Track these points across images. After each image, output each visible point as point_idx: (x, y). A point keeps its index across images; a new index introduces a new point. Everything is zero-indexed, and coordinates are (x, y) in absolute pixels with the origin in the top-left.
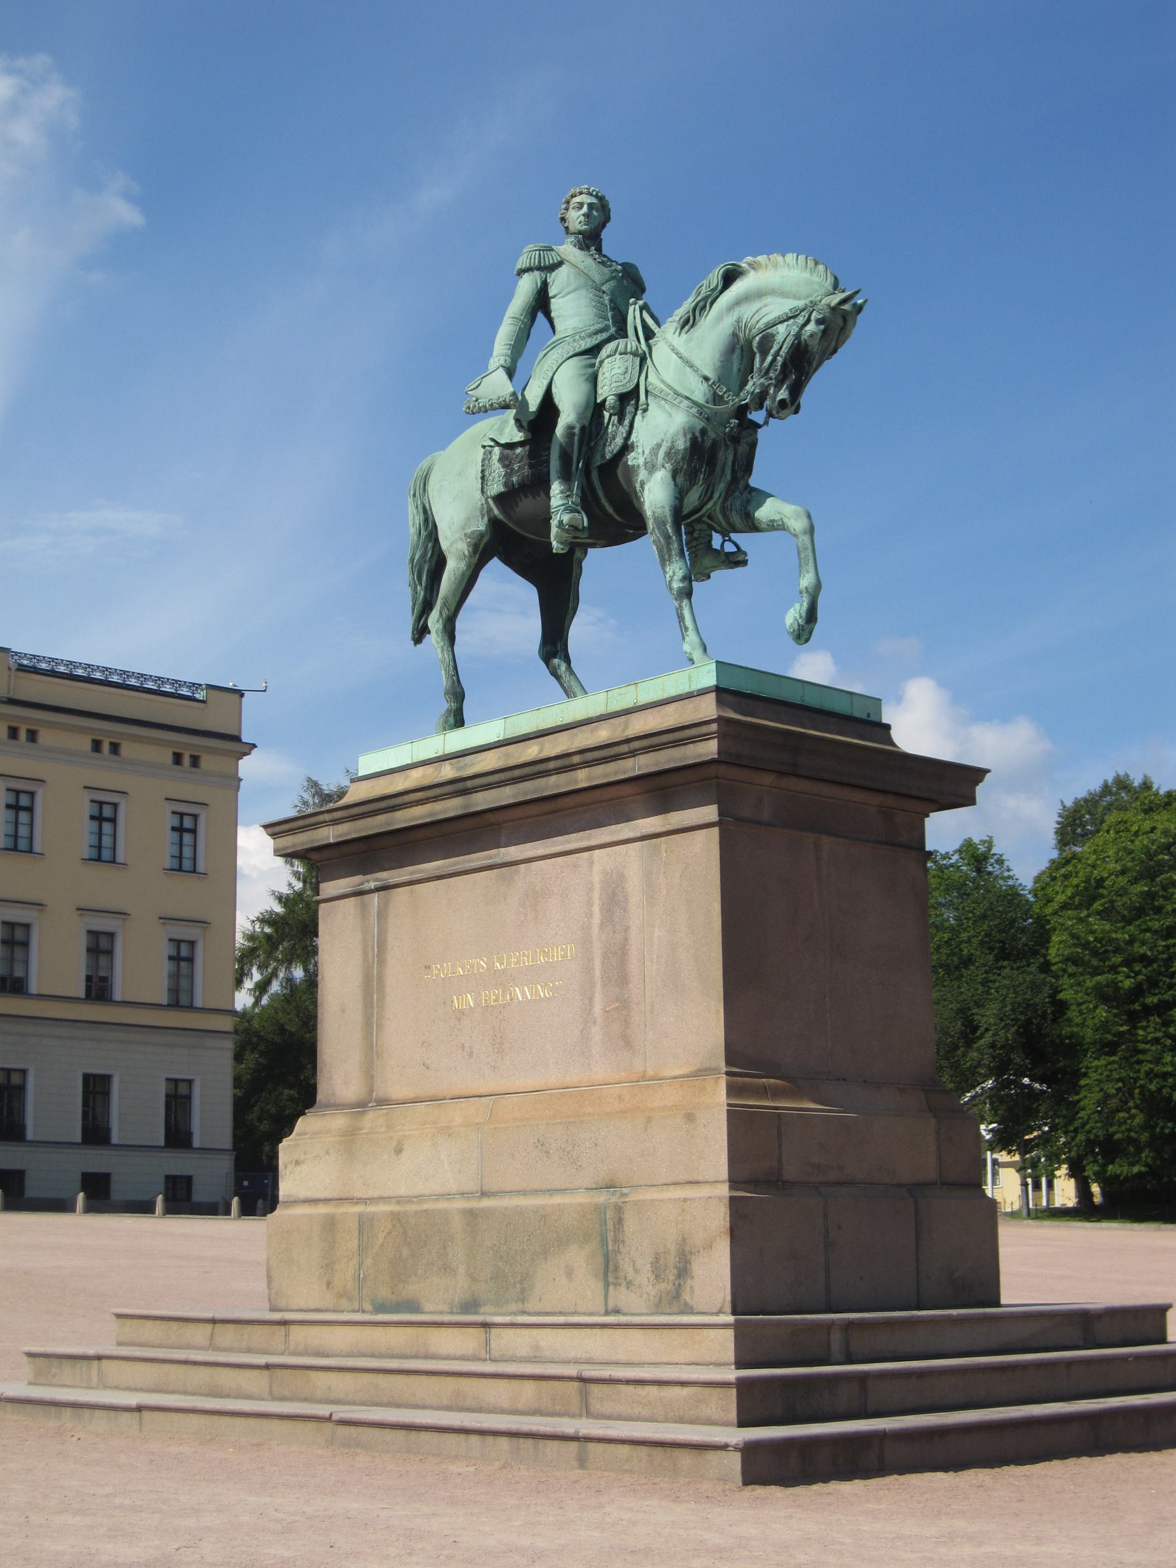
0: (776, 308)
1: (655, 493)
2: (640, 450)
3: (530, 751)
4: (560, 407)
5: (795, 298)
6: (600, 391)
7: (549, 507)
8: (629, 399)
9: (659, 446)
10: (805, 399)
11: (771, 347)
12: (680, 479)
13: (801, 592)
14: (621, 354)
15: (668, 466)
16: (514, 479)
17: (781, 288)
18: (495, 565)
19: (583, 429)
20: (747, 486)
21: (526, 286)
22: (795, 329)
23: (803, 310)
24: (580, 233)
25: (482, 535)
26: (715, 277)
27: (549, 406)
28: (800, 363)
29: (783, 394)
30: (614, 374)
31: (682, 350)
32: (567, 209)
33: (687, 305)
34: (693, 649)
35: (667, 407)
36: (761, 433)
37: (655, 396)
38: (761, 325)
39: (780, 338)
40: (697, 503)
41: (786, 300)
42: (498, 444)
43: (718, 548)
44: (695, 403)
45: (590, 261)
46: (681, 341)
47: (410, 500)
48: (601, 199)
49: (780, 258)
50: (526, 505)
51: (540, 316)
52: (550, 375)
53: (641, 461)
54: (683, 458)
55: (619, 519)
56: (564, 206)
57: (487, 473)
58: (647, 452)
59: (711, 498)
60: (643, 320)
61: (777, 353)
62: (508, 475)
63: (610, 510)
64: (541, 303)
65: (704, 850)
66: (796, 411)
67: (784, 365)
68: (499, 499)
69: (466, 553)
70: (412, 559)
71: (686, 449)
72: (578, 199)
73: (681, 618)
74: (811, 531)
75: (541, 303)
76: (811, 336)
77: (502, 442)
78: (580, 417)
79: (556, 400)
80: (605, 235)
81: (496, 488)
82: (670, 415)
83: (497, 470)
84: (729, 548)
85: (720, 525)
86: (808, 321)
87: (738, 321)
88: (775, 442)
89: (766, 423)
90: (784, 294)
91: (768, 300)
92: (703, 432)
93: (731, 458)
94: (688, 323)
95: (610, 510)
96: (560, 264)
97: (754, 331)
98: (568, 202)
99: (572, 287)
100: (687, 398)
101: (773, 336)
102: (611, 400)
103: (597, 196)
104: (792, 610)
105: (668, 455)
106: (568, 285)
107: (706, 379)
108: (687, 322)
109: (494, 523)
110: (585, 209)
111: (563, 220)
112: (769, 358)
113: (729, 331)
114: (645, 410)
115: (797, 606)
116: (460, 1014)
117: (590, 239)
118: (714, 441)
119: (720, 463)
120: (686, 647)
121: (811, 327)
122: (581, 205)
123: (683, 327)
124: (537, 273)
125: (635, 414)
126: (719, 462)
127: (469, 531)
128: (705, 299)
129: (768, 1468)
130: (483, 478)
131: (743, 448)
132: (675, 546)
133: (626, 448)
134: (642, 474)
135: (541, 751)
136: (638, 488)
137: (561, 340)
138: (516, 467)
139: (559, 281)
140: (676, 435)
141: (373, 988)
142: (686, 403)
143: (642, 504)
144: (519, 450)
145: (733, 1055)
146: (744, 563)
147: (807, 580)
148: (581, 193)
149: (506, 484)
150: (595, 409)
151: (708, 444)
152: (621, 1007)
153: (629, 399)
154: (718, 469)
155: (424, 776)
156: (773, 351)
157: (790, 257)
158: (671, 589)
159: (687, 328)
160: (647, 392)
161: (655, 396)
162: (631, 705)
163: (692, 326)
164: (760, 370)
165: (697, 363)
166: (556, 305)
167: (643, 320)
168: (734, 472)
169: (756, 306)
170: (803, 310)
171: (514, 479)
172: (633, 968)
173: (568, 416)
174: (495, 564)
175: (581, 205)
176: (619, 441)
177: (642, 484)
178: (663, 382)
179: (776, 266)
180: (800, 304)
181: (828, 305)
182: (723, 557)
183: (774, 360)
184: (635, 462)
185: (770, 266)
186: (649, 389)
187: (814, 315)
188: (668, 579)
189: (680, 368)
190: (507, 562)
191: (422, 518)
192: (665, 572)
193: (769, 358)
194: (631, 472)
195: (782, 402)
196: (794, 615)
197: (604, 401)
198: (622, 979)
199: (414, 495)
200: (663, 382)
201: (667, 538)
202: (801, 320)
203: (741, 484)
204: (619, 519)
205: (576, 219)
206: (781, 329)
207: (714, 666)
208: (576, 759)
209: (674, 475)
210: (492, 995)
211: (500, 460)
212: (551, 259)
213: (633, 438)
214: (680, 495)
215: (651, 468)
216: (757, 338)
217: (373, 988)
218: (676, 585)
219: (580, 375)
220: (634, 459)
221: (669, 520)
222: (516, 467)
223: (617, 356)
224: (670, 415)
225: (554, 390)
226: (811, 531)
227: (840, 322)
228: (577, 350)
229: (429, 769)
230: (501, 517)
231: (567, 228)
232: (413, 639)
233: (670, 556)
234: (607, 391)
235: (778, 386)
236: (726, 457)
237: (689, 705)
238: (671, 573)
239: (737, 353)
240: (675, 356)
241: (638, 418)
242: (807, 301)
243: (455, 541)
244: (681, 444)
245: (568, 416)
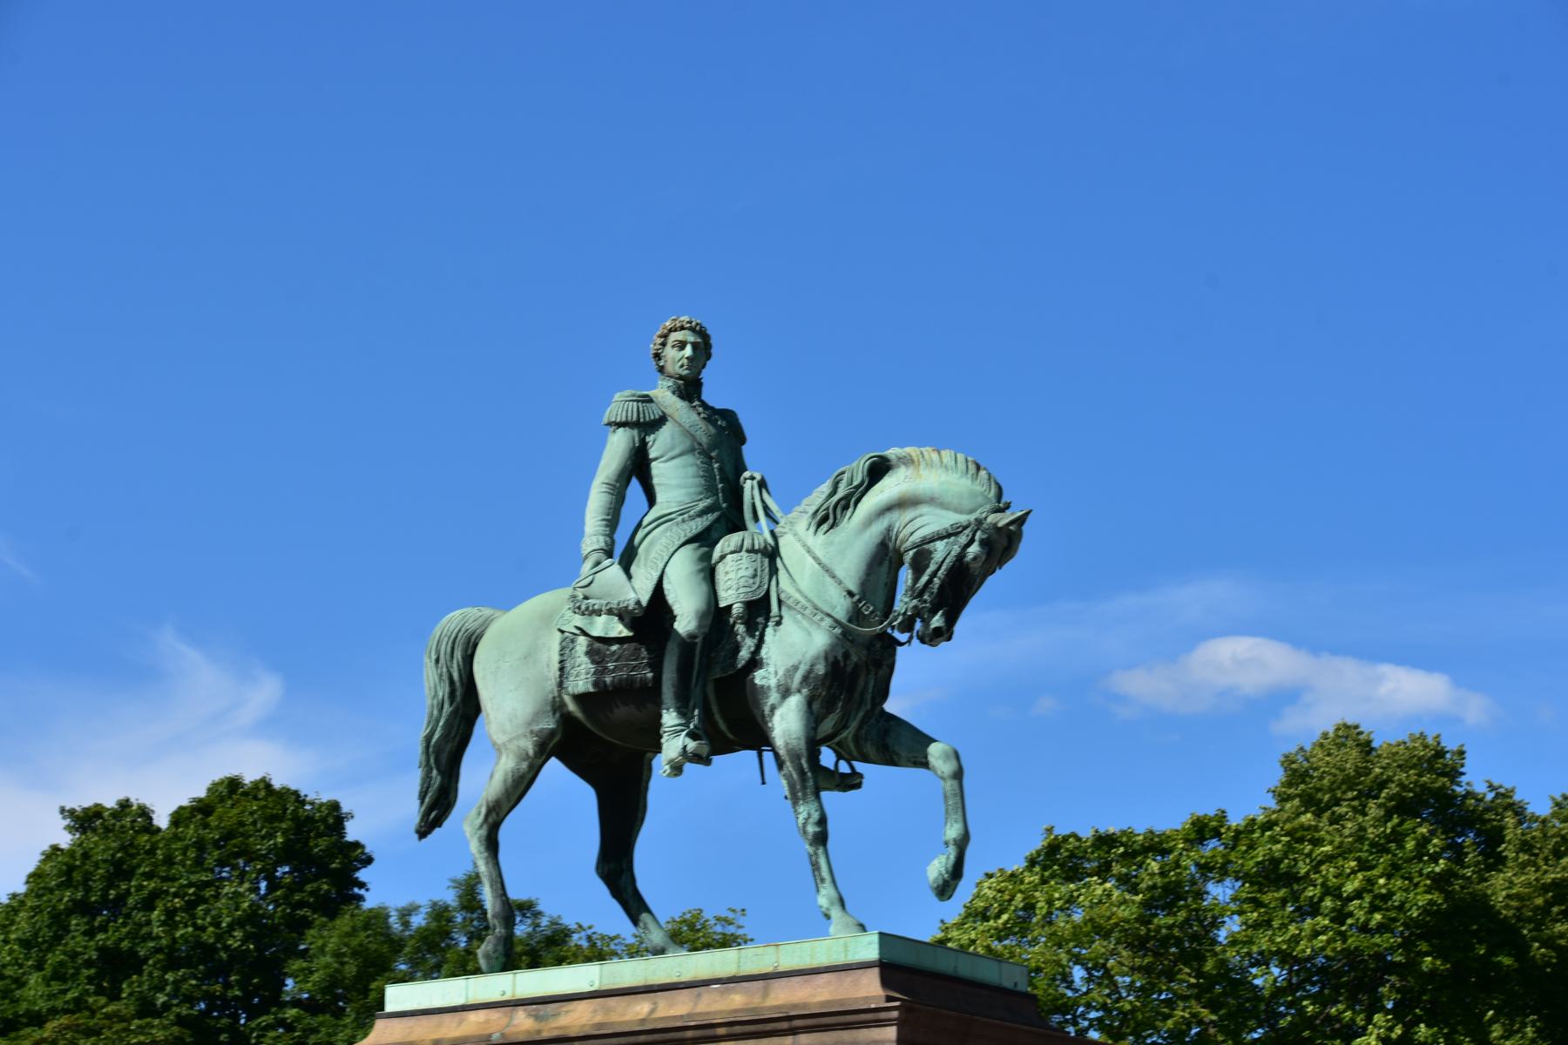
0: (929, 522)
1: (787, 722)
2: (771, 669)
3: (638, 1008)
4: (677, 610)
5: (956, 510)
6: (722, 593)
7: (660, 725)
8: (759, 611)
9: (796, 668)
10: (959, 627)
11: (927, 566)
12: (816, 706)
13: (947, 844)
14: (748, 551)
15: (805, 691)
16: (608, 679)
17: (934, 491)
18: (554, 766)
19: (706, 638)
20: (883, 711)
21: (618, 445)
22: (956, 550)
23: (965, 528)
24: (681, 377)
25: (552, 733)
26: (858, 469)
28: (956, 589)
29: (937, 621)
31: (819, 554)
32: (664, 344)
33: (819, 496)
34: (832, 904)
35: (805, 623)
36: (899, 649)
37: (790, 607)
38: (916, 537)
39: (938, 557)
40: (830, 731)
41: (944, 513)
42: (585, 633)
43: (832, 767)
44: (836, 621)
45: (694, 417)
46: (818, 541)
47: (429, 664)
48: (702, 333)
49: (935, 456)
50: (622, 712)
51: (635, 483)
52: (661, 566)
53: (773, 682)
54: (823, 684)
55: (731, 736)
56: (660, 341)
57: (568, 665)
58: (781, 673)
59: (845, 727)
60: (763, 501)
61: (934, 574)
62: (601, 671)
63: (723, 726)
64: (638, 466)
66: (949, 639)
67: (941, 587)
68: (580, 698)
69: (531, 752)
70: (428, 738)
71: (826, 674)
72: (675, 336)
73: (816, 867)
74: (958, 775)
75: (638, 466)
76: (975, 559)
77: (595, 633)
78: (700, 626)
79: (670, 598)
80: (706, 375)
82: (809, 634)
84: (844, 768)
85: (850, 753)
86: (971, 541)
87: (889, 529)
89: (909, 641)
90: (944, 506)
91: (924, 509)
92: (846, 656)
93: (871, 685)
94: (827, 519)
95: (723, 726)
96: (662, 420)
97: (908, 544)
98: (665, 336)
99: (677, 451)
100: (829, 615)
101: (930, 553)
102: (737, 609)
103: (692, 329)
104: (936, 862)
105: (806, 678)
106: (672, 448)
107: (851, 594)
108: (824, 519)
110: (688, 351)
111: (657, 356)
112: (925, 579)
113: (877, 540)
114: (778, 623)
115: (943, 859)
117: (689, 389)
118: (856, 665)
119: (859, 688)
120: (823, 901)
121: (974, 549)
122: (682, 345)
123: (819, 524)
124: (635, 432)
125: (766, 626)
126: (852, 686)
127: (536, 728)
128: (847, 498)
130: (562, 669)
131: (885, 669)
132: (811, 783)
133: (755, 663)
134: (774, 697)
135: (652, 1011)
136: (767, 710)
137: (663, 519)
138: (611, 665)
139: (659, 443)
140: (817, 658)
142: (828, 621)
143: (772, 729)
144: (614, 648)
146: (858, 786)
147: (953, 832)
148: (682, 328)
149: (595, 684)
150: (716, 615)
151: (849, 669)
154: (857, 695)
155: (487, 1021)
156: (929, 571)
157: (947, 455)
158: (805, 832)
159: (825, 527)
160: (780, 602)
161: (790, 607)
162: (770, 969)
163: (832, 527)
164: (912, 588)
165: (840, 574)
166: (656, 468)
167: (763, 501)
168: (873, 698)
169: (909, 514)
170: (965, 528)
171: (608, 679)
174: (554, 761)
175: (682, 345)
176: (744, 654)
177: (773, 708)
178: (799, 591)
179: (930, 465)
180: (964, 519)
181: (995, 525)
182: (837, 779)
183: (930, 581)
184: (763, 682)
185: (923, 465)
186: (783, 596)
187: (978, 535)
188: (801, 820)
189: (816, 570)
190: (559, 757)
191: (447, 689)
192: (797, 813)
193: (925, 579)
194: (759, 692)
195: (937, 629)
196: (937, 867)
197: (729, 607)
199: (437, 661)
200: (799, 591)
201: (802, 773)
202: (963, 539)
203: (877, 711)
204: (731, 736)
205: (676, 358)
206: (940, 546)
207: (876, 938)
208: (721, 1031)
209: (810, 702)
211: (588, 653)
212: (652, 413)
213: (763, 652)
215: (786, 693)
216: (911, 553)
218: (811, 829)
219: (701, 571)
220: (759, 677)
221: (804, 752)
222: (611, 665)
223: (743, 553)
224: (809, 634)
225: (666, 586)
226: (958, 775)
227: (1005, 542)
228: (690, 535)
229: (494, 1015)
230: (579, 714)
231: (661, 370)
232: (417, 832)
233: (805, 795)
235: (933, 612)
236: (868, 683)
237: (848, 978)
238: (804, 815)
239: (886, 564)
240: (810, 560)
241: (769, 631)
242: (972, 517)
243: (517, 738)
244: (821, 669)
245: (685, 623)
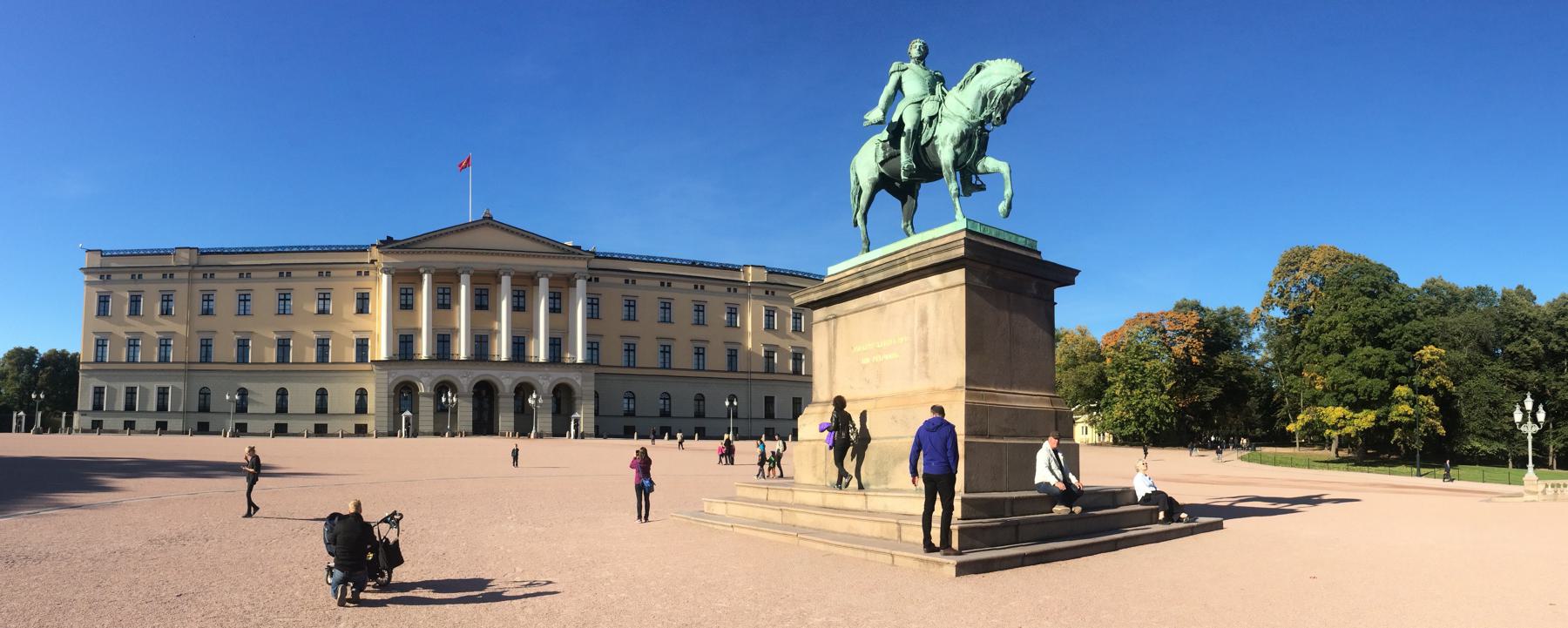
26: (973, 69)
27: (901, 122)
30: (928, 109)
65: (960, 295)
68: (882, 164)
81: (881, 159)
83: (881, 152)
88: (996, 135)
109: (881, 174)
116: (864, 367)
129: (963, 569)
133: (933, 138)
141: (832, 356)
143: (938, 161)
145: (968, 380)
152: (926, 360)
153: (933, 119)
172: (930, 346)
173: (909, 125)
198: (926, 350)
210: (877, 358)
214: (956, 156)
217: (832, 356)
234: (925, 116)
245: (909, 125)
